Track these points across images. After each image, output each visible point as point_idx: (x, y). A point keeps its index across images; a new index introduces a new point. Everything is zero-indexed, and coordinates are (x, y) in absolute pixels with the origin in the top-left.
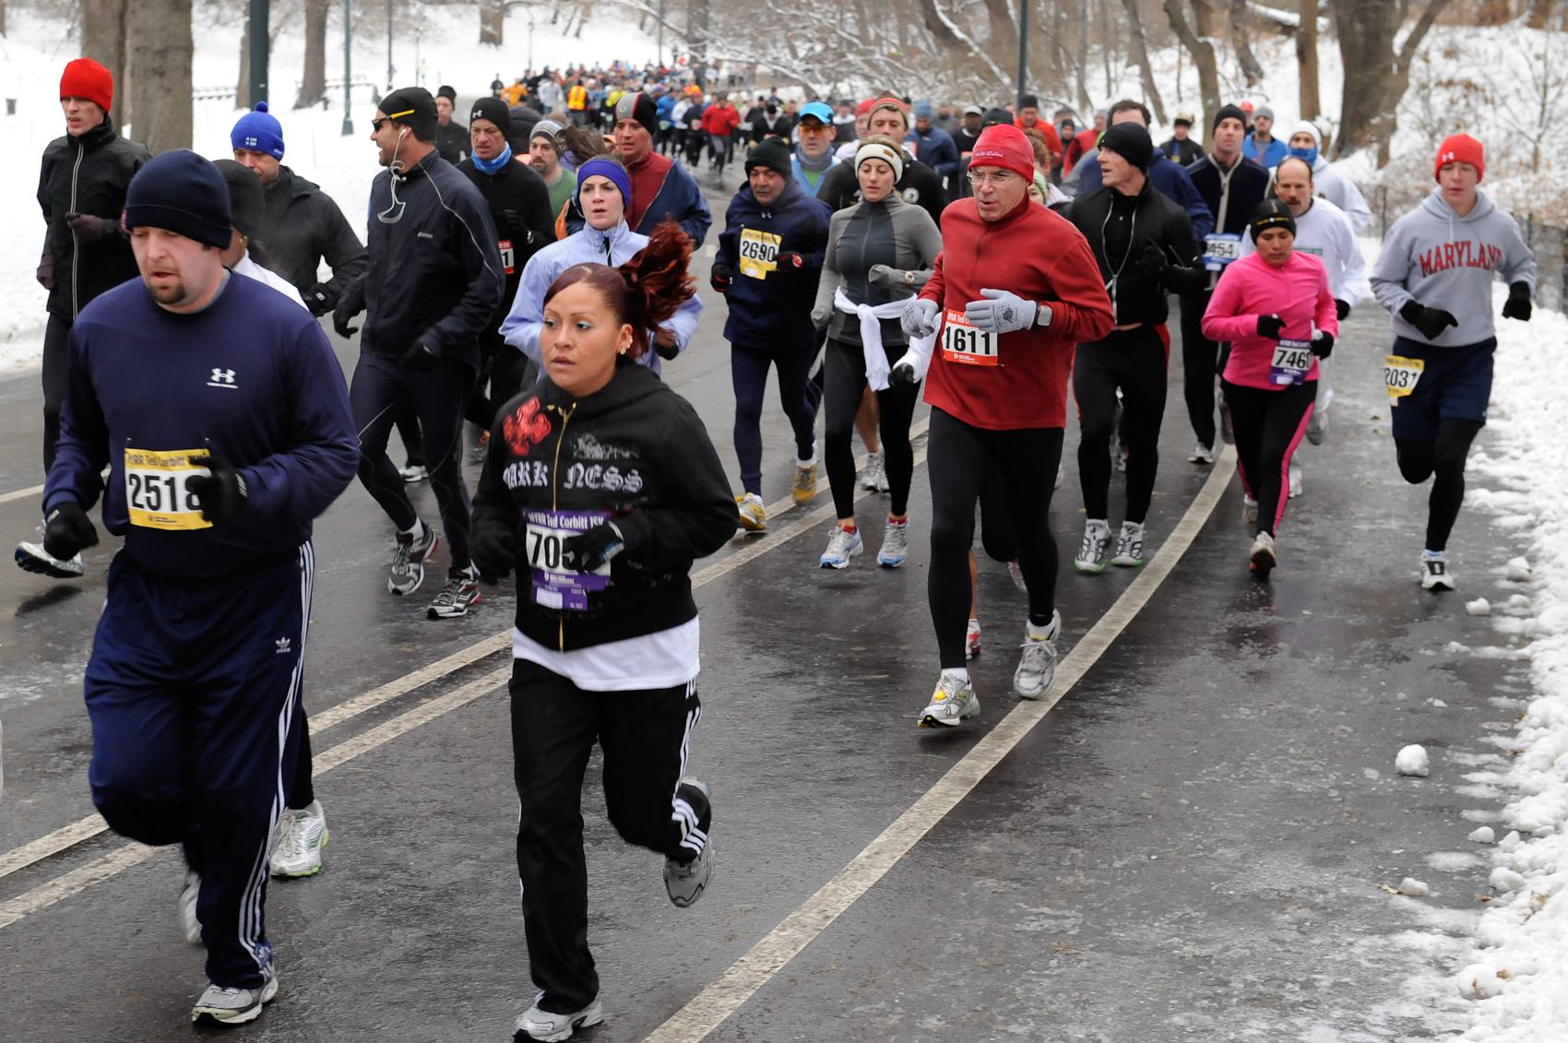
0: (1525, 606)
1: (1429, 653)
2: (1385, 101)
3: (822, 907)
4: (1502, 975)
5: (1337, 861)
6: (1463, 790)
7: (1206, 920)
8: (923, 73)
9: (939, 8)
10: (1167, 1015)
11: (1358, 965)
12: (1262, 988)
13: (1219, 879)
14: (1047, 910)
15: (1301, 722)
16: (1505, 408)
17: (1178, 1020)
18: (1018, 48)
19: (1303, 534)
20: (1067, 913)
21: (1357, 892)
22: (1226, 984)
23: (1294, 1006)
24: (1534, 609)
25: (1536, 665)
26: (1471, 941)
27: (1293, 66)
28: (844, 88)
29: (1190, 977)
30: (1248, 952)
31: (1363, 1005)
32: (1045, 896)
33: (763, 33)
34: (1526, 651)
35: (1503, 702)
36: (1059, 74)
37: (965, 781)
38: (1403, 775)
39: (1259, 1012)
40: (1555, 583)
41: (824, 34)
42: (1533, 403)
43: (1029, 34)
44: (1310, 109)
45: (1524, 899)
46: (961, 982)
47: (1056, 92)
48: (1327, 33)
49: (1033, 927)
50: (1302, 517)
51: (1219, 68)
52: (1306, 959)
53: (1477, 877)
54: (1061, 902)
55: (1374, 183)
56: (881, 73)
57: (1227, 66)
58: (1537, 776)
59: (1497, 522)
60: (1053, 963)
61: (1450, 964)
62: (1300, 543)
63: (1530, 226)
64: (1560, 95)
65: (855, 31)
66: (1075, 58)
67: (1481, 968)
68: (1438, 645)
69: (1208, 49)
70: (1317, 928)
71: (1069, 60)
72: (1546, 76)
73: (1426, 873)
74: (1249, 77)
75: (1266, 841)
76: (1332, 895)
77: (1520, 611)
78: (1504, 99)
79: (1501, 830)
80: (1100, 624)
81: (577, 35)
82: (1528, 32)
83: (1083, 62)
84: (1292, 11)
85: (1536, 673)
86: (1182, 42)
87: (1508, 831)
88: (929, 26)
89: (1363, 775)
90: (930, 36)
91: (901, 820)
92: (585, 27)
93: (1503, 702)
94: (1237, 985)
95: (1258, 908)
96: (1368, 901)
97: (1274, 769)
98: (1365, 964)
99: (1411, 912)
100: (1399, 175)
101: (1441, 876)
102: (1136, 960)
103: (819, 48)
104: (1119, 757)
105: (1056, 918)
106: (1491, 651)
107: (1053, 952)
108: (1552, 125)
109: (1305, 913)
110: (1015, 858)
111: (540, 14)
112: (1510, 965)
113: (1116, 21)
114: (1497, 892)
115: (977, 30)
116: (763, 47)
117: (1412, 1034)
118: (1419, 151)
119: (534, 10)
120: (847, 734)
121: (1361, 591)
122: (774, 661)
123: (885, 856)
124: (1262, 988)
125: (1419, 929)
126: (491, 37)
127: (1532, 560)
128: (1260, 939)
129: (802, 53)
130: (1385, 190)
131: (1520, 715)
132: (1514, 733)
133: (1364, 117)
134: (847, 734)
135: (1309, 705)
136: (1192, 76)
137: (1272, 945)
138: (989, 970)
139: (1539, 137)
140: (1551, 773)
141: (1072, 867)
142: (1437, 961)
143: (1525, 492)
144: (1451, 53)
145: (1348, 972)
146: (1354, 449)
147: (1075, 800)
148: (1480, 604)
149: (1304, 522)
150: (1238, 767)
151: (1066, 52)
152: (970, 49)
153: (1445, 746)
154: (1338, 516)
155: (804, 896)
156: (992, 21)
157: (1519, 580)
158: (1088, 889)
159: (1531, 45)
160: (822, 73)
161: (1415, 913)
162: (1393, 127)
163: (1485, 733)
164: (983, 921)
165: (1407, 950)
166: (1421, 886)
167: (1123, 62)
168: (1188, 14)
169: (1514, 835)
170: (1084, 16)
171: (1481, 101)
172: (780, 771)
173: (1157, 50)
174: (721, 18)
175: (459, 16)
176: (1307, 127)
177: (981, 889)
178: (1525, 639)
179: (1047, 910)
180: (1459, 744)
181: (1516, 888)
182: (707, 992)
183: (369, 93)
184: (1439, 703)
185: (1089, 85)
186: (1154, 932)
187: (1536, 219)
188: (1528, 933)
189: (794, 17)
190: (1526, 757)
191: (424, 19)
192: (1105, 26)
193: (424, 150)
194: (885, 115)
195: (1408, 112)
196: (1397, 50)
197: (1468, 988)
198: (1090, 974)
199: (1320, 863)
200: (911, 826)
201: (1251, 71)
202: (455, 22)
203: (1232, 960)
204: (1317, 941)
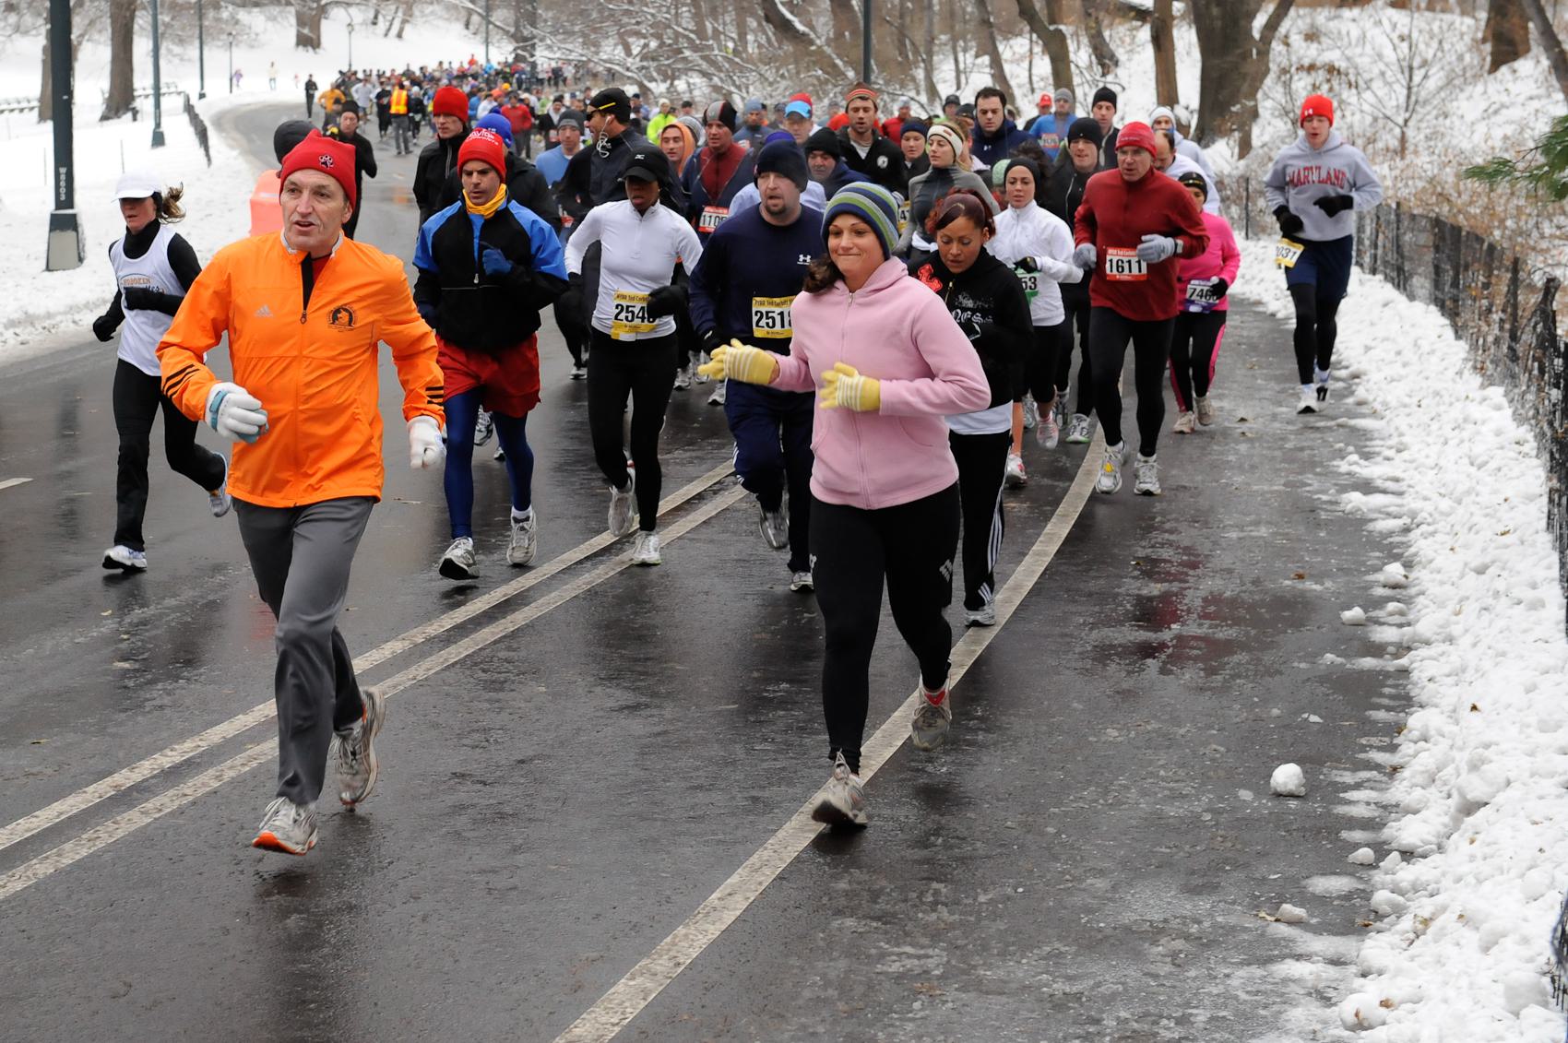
0: (1402, 614)
1: (1303, 665)
2: (1245, 88)
3: (672, 953)
4: (1385, 1004)
5: (1211, 888)
6: (1341, 810)
7: (1076, 954)
8: (763, 68)
11: (1236, 998)
12: (1136, 1025)
13: (1089, 911)
14: (908, 949)
15: (1170, 742)
16: (1377, 406)
18: (861, 41)
20: (930, 952)
21: (1233, 920)
22: (1098, 1022)
24: (1411, 617)
25: (1415, 676)
26: (1353, 969)
27: (1149, 51)
28: (681, 85)
29: (1060, 1016)
30: (1121, 988)
32: (907, 934)
33: (595, 30)
34: (1404, 661)
35: (1381, 715)
36: (906, 66)
38: (1279, 795)
40: (1433, 590)
41: (659, 29)
42: (1407, 400)
43: (873, 25)
44: (1168, 94)
45: (1407, 923)
46: (821, 1029)
47: (903, 86)
48: (1183, 17)
49: (895, 968)
50: (1167, 526)
51: (1072, 56)
52: (1181, 994)
53: (1357, 902)
54: (925, 941)
55: (1236, 173)
57: (1080, 55)
58: (1418, 792)
59: (1371, 526)
60: (917, 1005)
61: (1331, 993)
62: (1166, 553)
63: (1398, 215)
64: (1426, 77)
65: (692, 26)
66: (922, 49)
67: (1363, 998)
68: (1313, 657)
69: (1061, 37)
70: (1192, 959)
71: (916, 52)
72: (1411, 58)
73: (1305, 899)
74: (1103, 65)
75: (1137, 869)
77: (1397, 619)
78: (1368, 83)
79: (1381, 850)
81: (399, 36)
82: (1391, 12)
83: (930, 54)
85: (1415, 684)
86: (1032, 30)
87: (1389, 852)
88: (768, 19)
89: (1237, 797)
90: (770, 29)
91: (754, 859)
92: (408, 27)
93: (1381, 715)
94: (1110, 1022)
95: (1130, 941)
96: (1245, 930)
98: (1243, 996)
99: (1290, 940)
101: (1321, 901)
102: (1004, 999)
103: (653, 44)
104: (981, 785)
105: (919, 957)
106: (1368, 662)
108: (1418, 108)
109: (1179, 944)
110: (875, 896)
111: (359, 15)
112: (1395, 994)
113: (964, 10)
114: (1380, 917)
115: (820, 26)
116: (596, 45)
119: (353, 11)
120: (697, 769)
121: (1234, 602)
122: (618, 693)
123: (738, 897)
124: (1136, 1025)
125: (1298, 957)
126: (308, 40)
127: (1408, 565)
128: (1133, 973)
129: (635, 50)
130: (1247, 180)
131: (1399, 728)
132: (1393, 748)
133: (1225, 102)
134: (697, 769)
136: (1043, 66)
137: (1144, 979)
138: (850, 1014)
139: (1406, 121)
140: (1433, 789)
141: (936, 903)
142: (1317, 991)
143: (1400, 494)
144: (1312, 36)
146: (1222, 453)
147: (937, 833)
148: (1355, 613)
149: (1171, 532)
150: (1106, 792)
151: (913, 44)
152: (812, 42)
153: (1322, 764)
154: (1206, 524)
155: (654, 941)
156: (833, 11)
157: (1395, 587)
158: (952, 926)
159: (1394, 26)
160: (658, 70)
161: (1293, 941)
162: (1255, 114)
163: (1363, 749)
164: (843, 964)
165: (1286, 981)
166: (1299, 912)
167: (973, 52)
169: (1395, 855)
171: (1345, 86)
172: (627, 810)
173: (1007, 39)
174: (550, 14)
175: (273, 19)
176: (1164, 111)
177: (840, 930)
178: (1404, 649)
179: (908, 949)
180: (1337, 761)
181: (1399, 911)
183: (180, 101)
184: (1314, 718)
185: (937, 77)
186: (1022, 969)
187: (1404, 208)
188: (1412, 959)
189: (627, 12)
190: (1406, 773)
191: (237, 22)
192: (952, 14)
193: (621, 128)
194: (859, 103)
195: (1270, 99)
196: (1256, 35)
197: (1351, 1019)
198: (955, 1016)
199: (1194, 891)
200: (765, 864)
201: (1105, 59)
202: (270, 24)
203: (1103, 996)
204: (1192, 973)
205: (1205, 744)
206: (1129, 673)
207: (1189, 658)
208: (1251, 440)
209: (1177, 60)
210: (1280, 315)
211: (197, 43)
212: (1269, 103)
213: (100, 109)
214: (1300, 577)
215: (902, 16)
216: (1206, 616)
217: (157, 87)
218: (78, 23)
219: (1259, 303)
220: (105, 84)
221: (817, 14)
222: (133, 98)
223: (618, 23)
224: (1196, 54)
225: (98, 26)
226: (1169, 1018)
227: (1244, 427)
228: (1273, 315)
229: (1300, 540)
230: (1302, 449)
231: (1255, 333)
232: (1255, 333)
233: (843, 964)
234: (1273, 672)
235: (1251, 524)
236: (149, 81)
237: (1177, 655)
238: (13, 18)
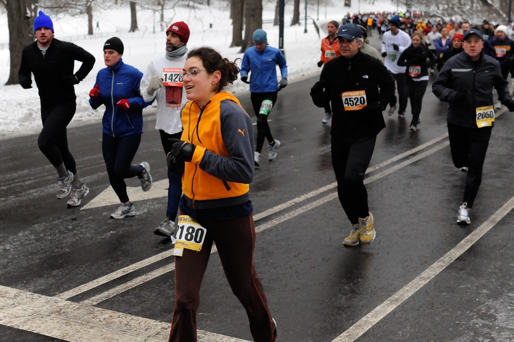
37: (493, 221)
46: (493, 280)
138: (503, 276)
182: (416, 279)
183: (312, 21)
233: (500, 263)
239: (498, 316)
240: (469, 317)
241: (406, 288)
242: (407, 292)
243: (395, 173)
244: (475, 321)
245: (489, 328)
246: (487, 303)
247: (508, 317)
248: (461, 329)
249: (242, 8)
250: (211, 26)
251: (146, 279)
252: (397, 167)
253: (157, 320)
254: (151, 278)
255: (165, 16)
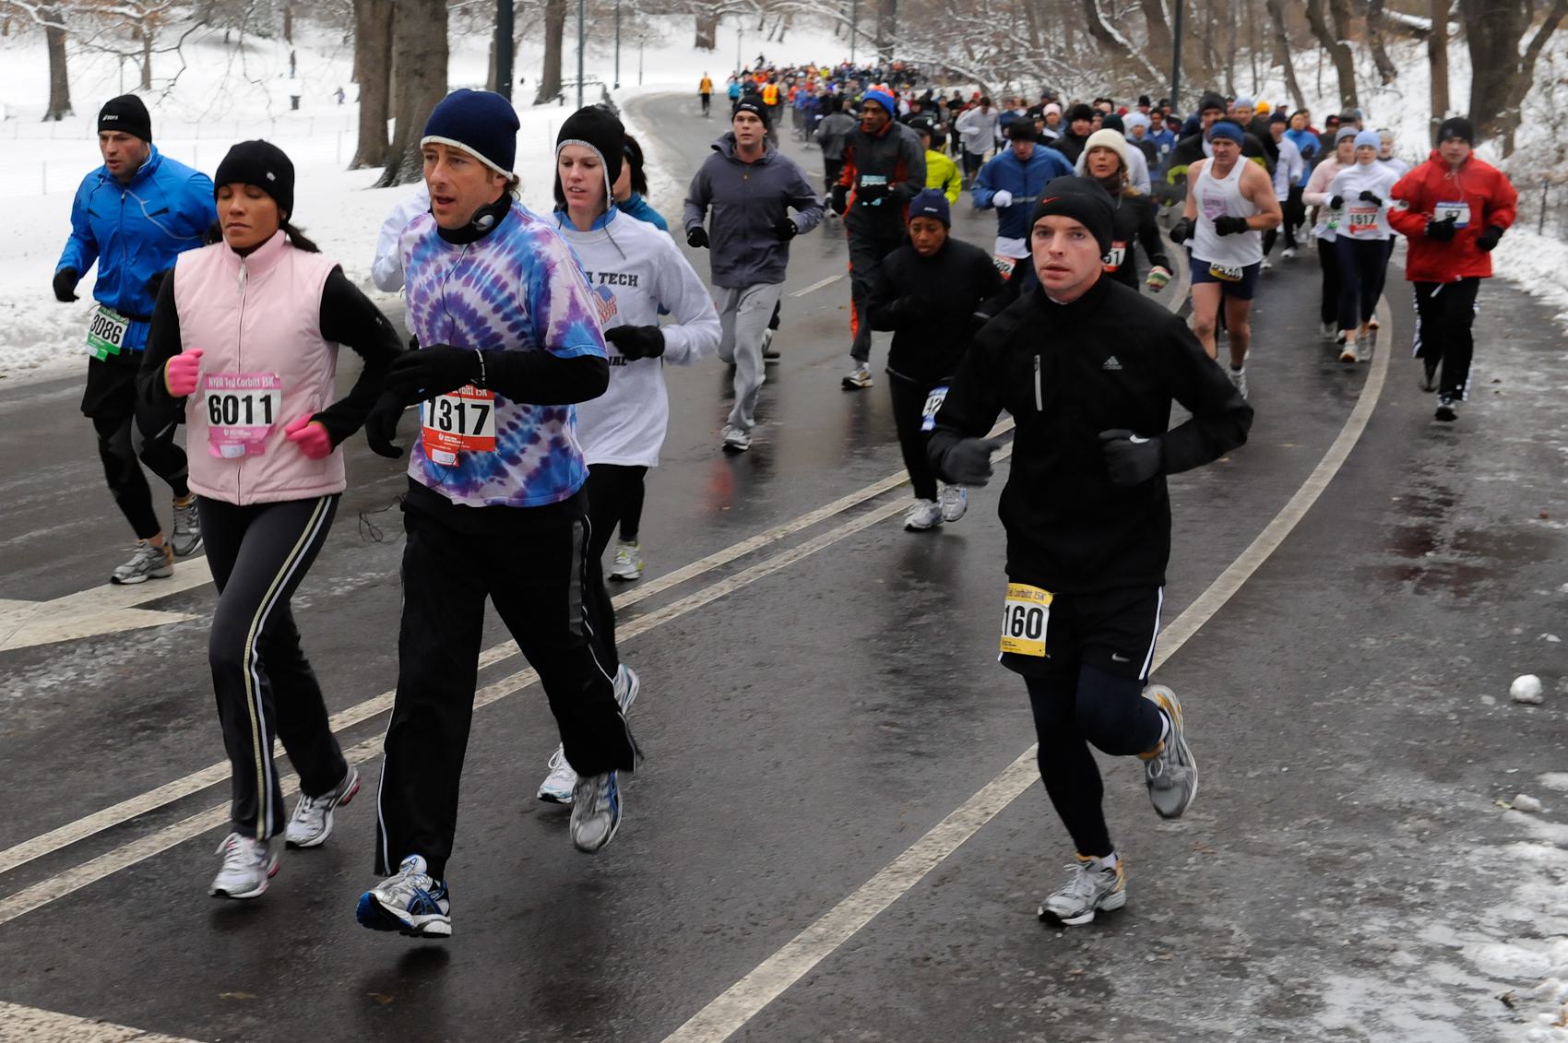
1: (1544, 593)
2: (1510, 97)
7: (1332, 827)
9: (1101, 15)
10: (1296, 910)
11: (1474, 872)
12: (1383, 890)
13: (1345, 790)
15: (1422, 653)
17: (1305, 915)
18: (1172, 51)
19: (1427, 484)
21: (1473, 806)
23: (1413, 906)
27: (1424, 68)
28: (1015, 85)
31: (1478, 907)
33: (945, 38)
38: (1519, 702)
39: (1381, 911)
41: (998, 38)
43: (1183, 37)
48: (1457, 36)
51: (1356, 68)
52: (1425, 865)
56: (1049, 73)
60: (1191, 860)
61: (1559, 873)
65: (1026, 36)
70: (1435, 837)
71: (1219, 62)
73: (1537, 791)
75: (1386, 759)
76: (1449, 808)
80: (1239, 561)
81: (780, 40)
83: (1231, 63)
84: (1425, 17)
86: (1323, 45)
88: (1092, 31)
90: (1093, 41)
92: (788, 34)
94: (1360, 885)
95: (1381, 818)
96: (1484, 815)
97: (1398, 694)
98: (1480, 871)
99: (1524, 826)
100: (1524, 163)
102: (1268, 860)
103: (993, 51)
107: (1189, 851)
109: (1424, 823)
111: (747, 22)
115: (1136, 38)
116: (945, 50)
117: (1524, 936)
118: (1543, 142)
119: (743, 19)
121: (1483, 536)
125: (1531, 841)
126: (706, 43)
129: (978, 56)
135: (1431, 637)
136: (1331, 75)
145: (1463, 878)
149: (1429, 474)
150: (1363, 690)
151: (1217, 54)
152: (1129, 52)
153: (1559, 677)
154: (1460, 469)
156: (1149, 26)
162: (1517, 121)
165: (1519, 860)
166: (1533, 802)
167: (1269, 63)
168: (1328, 20)
170: (1233, 22)
175: (676, 24)
182: (880, 876)
184: (1552, 638)
186: (1285, 836)
189: (972, 24)
195: (1532, 107)
196: (1522, 52)
204: (1435, 849)
205: (1453, 655)
206: (1387, 592)
207: (1441, 581)
208: (1504, 398)
209: (1450, 72)
210: (1534, 293)
211: (614, 43)
212: (1531, 111)
213: (534, 96)
214: (1544, 517)
215: (1208, 31)
216: (1456, 546)
217: (580, 78)
218: (519, 25)
219: (1515, 282)
220: (539, 75)
221: (1136, 28)
222: (560, 87)
223: (963, 32)
224: (1468, 68)
225: (535, 27)
226: (1413, 885)
227: (1498, 387)
228: (1527, 293)
229: (1545, 486)
230: (1549, 408)
231: (1510, 307)
232: (1510, 307)
234: (1515, 597)
235: (1501, 470)
236: (575, 73)
237: (1431, 580)
238: (467, 20)
239: (1118, 985)
240: (1032, 987)
241: (849, 903)
242: (854, 914)
243: (832, 550)
244: (1050, 1000)
245: (1089, 1022)
246: (1085, 946)
247: (1148, 986)
248: (1009, 1025)
249: (388, 50)
250: (295, 102)
251: (61, 889)
252: (838, 533)
253: (89, 1016)
254: (76, 887)
255: (155, 74)
